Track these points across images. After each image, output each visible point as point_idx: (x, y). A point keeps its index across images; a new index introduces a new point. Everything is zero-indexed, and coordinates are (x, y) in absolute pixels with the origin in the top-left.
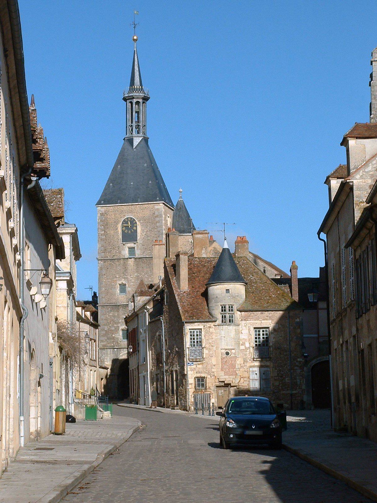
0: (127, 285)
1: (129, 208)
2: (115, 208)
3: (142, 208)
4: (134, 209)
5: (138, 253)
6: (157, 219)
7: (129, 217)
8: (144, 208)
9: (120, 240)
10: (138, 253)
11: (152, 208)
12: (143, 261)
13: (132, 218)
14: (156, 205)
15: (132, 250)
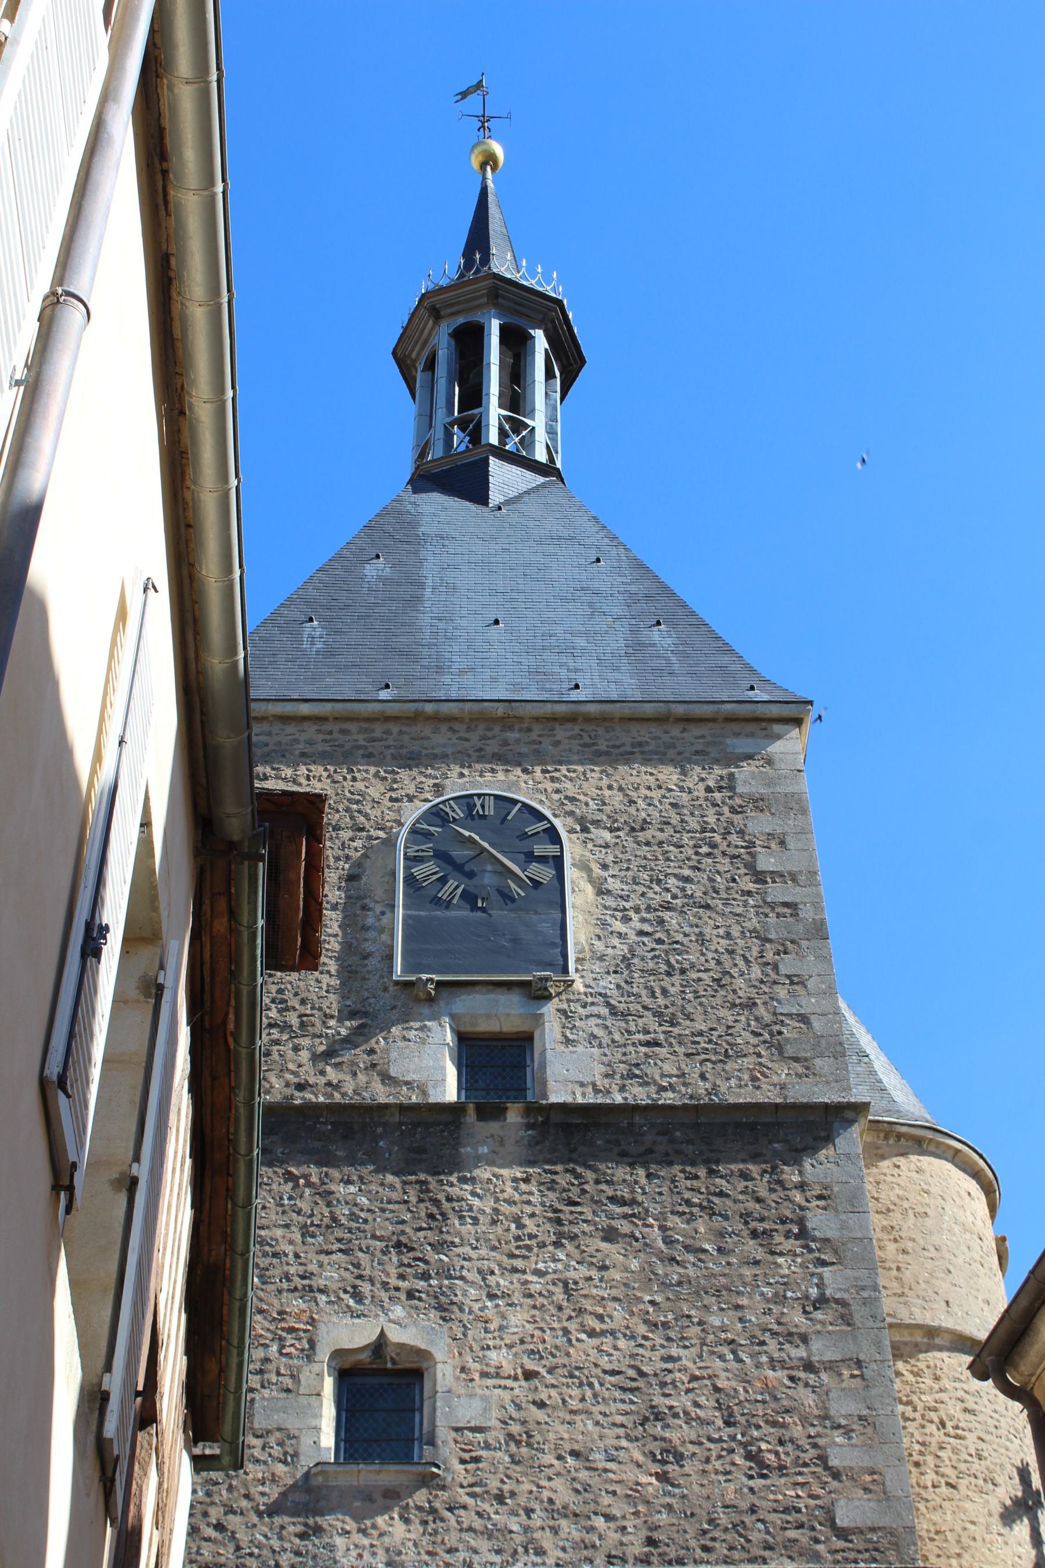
0: (444, 1373)
1: (483, 738)
2: (343, 732)
3: (603, 746)
4: (525, 750)
5: (570, 1071)
6: (759, 824)
7: (479, 796)
8: (628, 749)
9: (373, 962)
10: (570, 1071)
11: (699, 747)
12: (633, 1149)
13: (515, 802)
14: (737, 735)
15: (497, 1063)
